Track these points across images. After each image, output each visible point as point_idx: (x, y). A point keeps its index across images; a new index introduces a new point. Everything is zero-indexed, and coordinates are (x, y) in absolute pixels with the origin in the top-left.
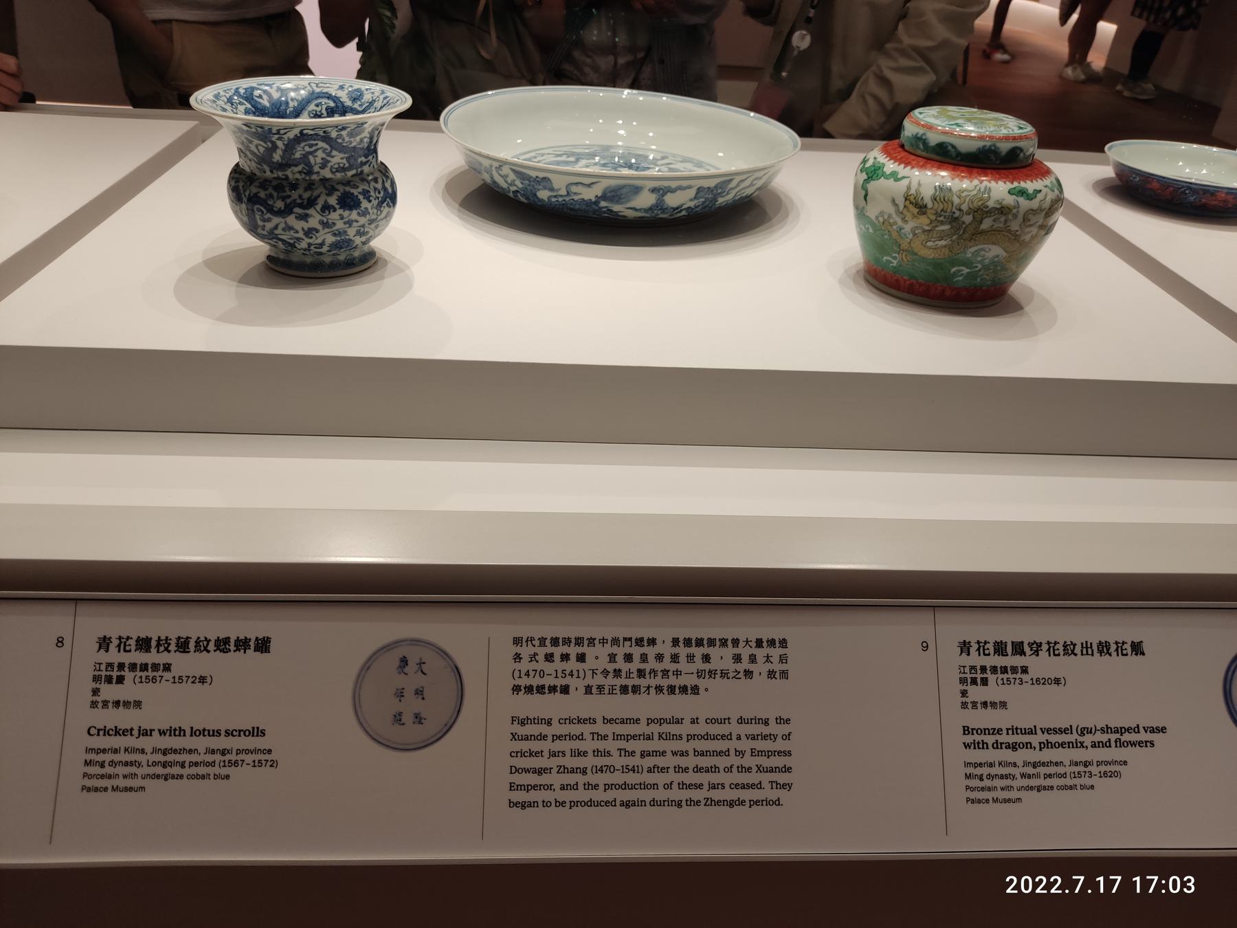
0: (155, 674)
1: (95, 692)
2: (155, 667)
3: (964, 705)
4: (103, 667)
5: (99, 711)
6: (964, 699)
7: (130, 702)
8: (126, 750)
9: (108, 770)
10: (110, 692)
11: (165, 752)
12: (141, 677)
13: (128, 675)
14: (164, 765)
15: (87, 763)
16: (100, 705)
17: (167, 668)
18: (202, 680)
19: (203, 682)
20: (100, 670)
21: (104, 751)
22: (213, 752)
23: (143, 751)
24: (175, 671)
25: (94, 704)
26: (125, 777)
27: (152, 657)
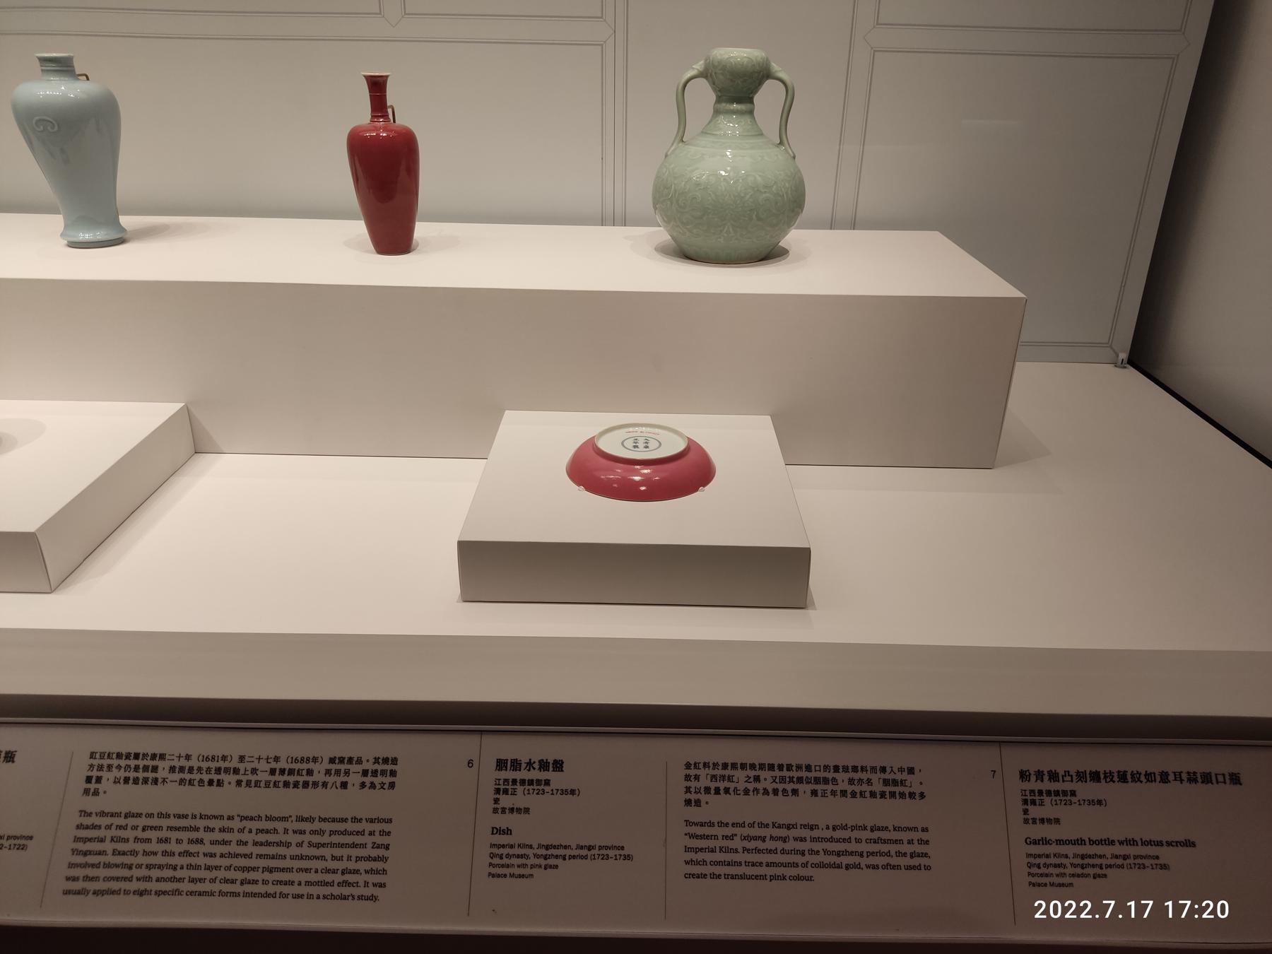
0: (538, 787)
1: (496, 801)
2: (539, 782)
3: (1026, 821)
4: (501, 782)
5: (499, 816)
6: (1026, 817)
7: (521, 809)
8: (519, 846)
9: (506, 861)
10: (506, 801)
11: (547, 847)
12: (529, 790)
13: (519, 788)
14: (546, 858)
15: (492, 856)
16: (500, 811)
17: (547, 783)
18: (573, 792)
19: (573, 794)
20: (499, 785)
21: (503, 846)
22: (582, 848)
23: (531, 847)
24: (553, 785)
25: (495, 811)
26: (519, 866)
27: (535, 774)
